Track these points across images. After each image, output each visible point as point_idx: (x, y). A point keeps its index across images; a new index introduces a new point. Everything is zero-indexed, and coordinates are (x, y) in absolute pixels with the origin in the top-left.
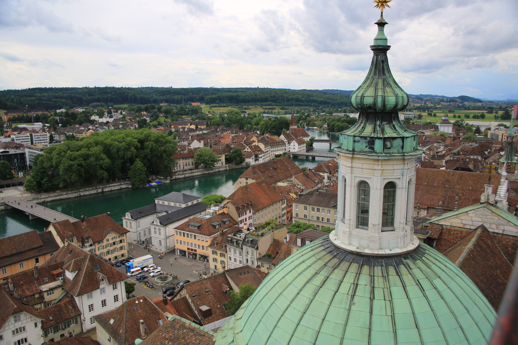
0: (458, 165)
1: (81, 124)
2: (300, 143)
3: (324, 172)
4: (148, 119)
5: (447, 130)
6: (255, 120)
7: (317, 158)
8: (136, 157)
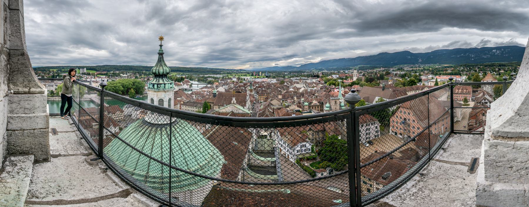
0: (236, 91)
1: (117, 76)
2: (187, 85)
3: (194, 95)
4: (138, 76)
5: (235, 80)
6: (173, 77)
7: (193, 90)
8: (132, 88)
